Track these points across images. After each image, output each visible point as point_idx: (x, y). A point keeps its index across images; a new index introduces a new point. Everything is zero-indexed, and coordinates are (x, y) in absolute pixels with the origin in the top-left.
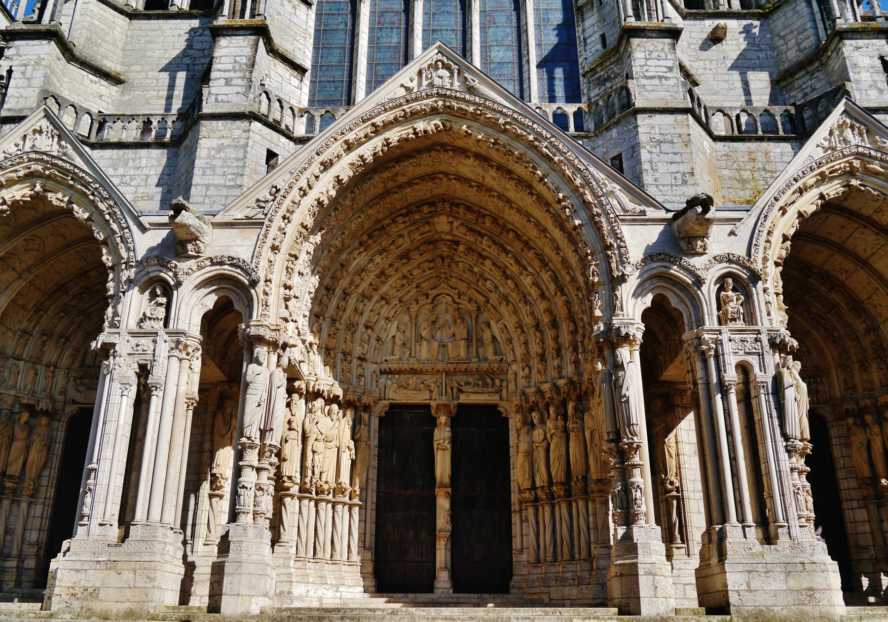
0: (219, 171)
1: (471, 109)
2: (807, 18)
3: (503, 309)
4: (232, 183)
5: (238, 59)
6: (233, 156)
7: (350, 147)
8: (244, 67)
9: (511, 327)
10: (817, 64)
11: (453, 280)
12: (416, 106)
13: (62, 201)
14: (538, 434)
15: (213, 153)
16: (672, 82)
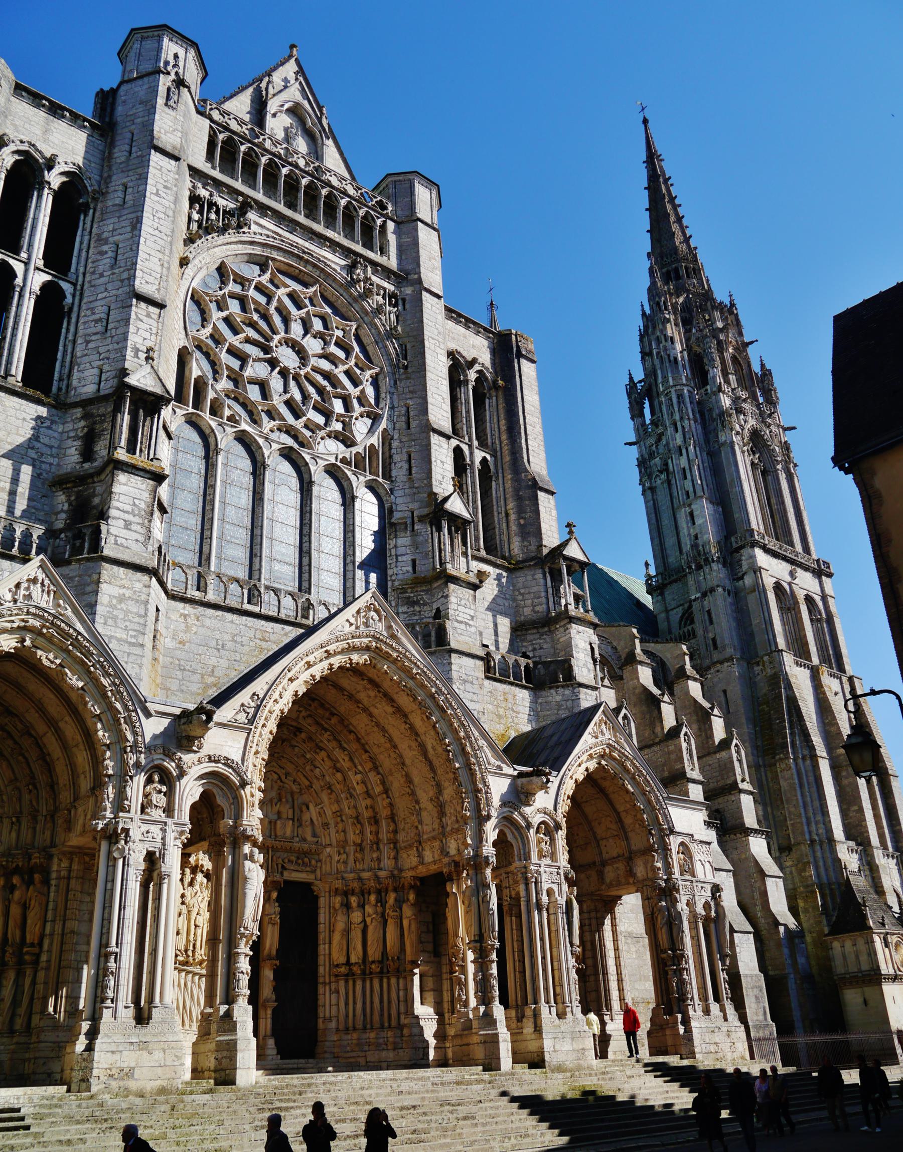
0: (121, 624)
1: (395, 655)
2: (542, 588)
3: (324, 796)
4: (134, 640)
5: (137, 502)
6: (135, 610)
7: (309, 665)
8: (143, 513)
9: (329, 813)
10: (546, 629)
11: (284, 760)
12: (357, 641)
13: (52, 662)
14: (356, 917)
15: (114, 601)
16: (473, 629)
